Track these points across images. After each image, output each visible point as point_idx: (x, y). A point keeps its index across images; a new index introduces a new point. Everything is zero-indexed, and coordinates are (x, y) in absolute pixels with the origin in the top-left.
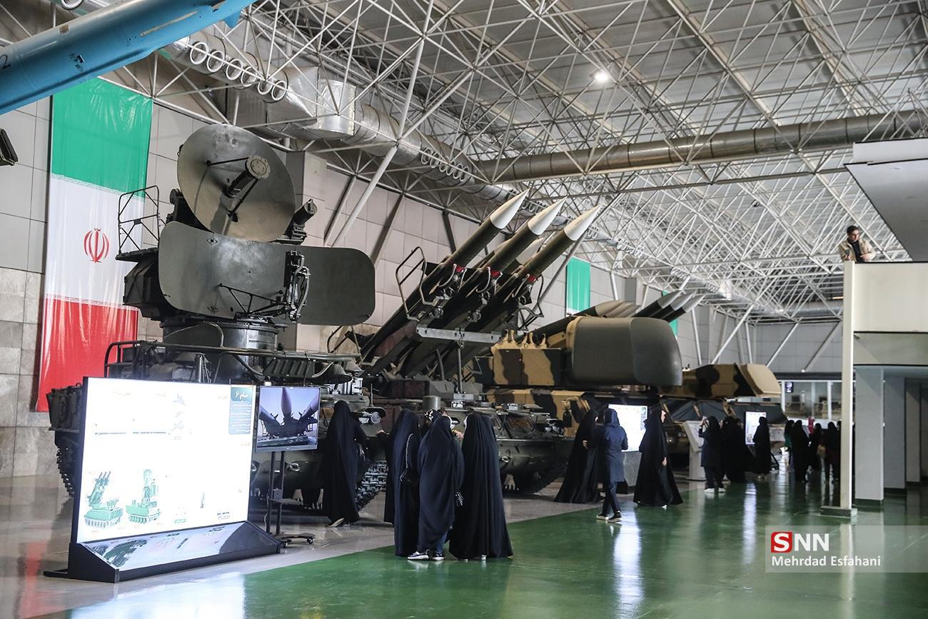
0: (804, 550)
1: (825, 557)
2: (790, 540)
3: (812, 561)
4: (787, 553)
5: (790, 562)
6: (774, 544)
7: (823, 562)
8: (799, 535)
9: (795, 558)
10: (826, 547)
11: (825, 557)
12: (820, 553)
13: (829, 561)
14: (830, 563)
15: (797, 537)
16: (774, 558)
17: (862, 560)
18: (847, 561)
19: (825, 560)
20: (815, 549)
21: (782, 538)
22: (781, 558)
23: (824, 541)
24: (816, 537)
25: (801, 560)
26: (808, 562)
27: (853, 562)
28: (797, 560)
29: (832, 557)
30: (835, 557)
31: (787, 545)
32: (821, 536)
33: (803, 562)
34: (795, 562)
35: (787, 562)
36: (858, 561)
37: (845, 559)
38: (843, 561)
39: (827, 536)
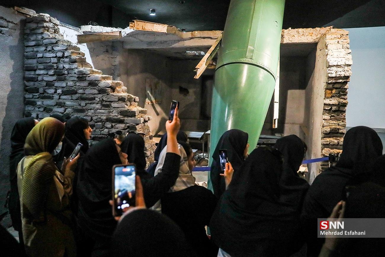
0: (333, 228)
1: (342, 231)
2: (328, 224)
3: (337, 233)
7: (341, 233)
9: (330, 232)
10: (343, 227)
11: (342, 231)
12: (340, 230)
13: (344, 233)
15: (331, 223)
16: (321, 232)
18: (352, 233)
19: (342, 233)
20: (338, 228)
21: (324, 223)
22: (324, 232)
24: (339, 223)
25: (332, 233)
26: (335, 233)
27: (354, 233)
29: (345, 231)
30: (347, 231)
33: (333, 233)
34: (330, 233)
36: (356, 233)
37: (351, 232)
38: (350, 233)
39: (343, 223)
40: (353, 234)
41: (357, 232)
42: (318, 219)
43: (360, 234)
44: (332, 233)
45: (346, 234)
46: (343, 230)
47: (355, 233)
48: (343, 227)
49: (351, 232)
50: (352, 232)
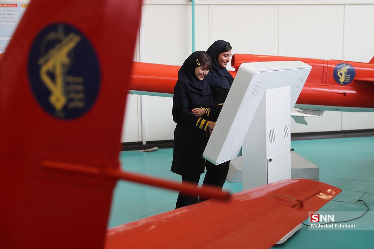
2: (318, 217)
3: (327, 226)
4: (317, 223)
6: (312, 219)
7: (332, 226)
8: (322, 215)
13: (334, 226)
15: (321, 216)
17: (347, 225)
18: (341, 226)
20: (329, 221)
21: (315, 216)
24: (329, 216)
26: (326, 226)
27: (344, 226)
30: (337, 224)
31: (317, 219)
32: (331, 215)
33: (324, 226)
36: (346, 226)
37: (341, 225)
38: (340, 226)
39: (333, 216)
40: (343, 227)
41: (347, 225)
42: (309, 212)
43: (349, 226)
45: (336, 226)
47: (345, 225)
49: (341, 225)
50: (342, 225)
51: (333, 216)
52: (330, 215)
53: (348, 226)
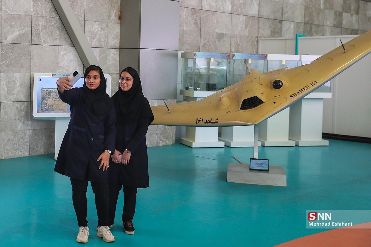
0: (322, 219)
1: (330, 222)
2: (316, 216)
3: (325, 224)
5: (316, 224)
6: (309, 217)
7: (329, 224)
9: (318, 223)
10: (330, 218)
11: (330, 222)
12: (328, 221)
14: (332, 225)
16: (309, 223)
19: (330, 223)
20: (326, 219)
21: (313, 215)
22: (312, 223)
23: (329, 215)
24: (326, 214)
25: (320, 224)
26: (323, 224)
27: (341, 224)
28: (318, 223)
29: (333, 222)
30: (334, 222)
31: (314, 217)
33: (321, 224)
34: (318, 224)
35: (315, 224)
36: (343, 224)
37: (338, 223)
38: (337, 224)
39: (331, 214)
41: (344, 223)
43: (346, 224)
44: (320, 224)
45: (333, 225)
46: (330, 221)
47: (342, 223)
48: (330, 218)
49: (338, 223)
51: (331, 214)
52: (327, 213)
53: (345, 224)
